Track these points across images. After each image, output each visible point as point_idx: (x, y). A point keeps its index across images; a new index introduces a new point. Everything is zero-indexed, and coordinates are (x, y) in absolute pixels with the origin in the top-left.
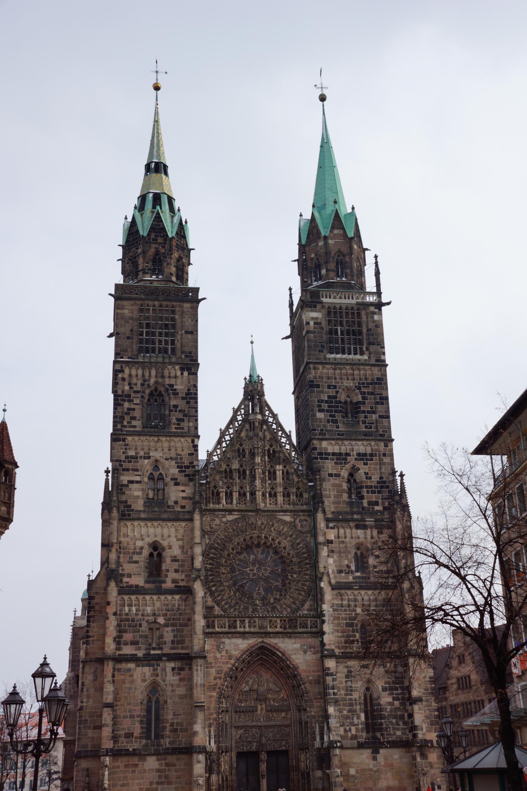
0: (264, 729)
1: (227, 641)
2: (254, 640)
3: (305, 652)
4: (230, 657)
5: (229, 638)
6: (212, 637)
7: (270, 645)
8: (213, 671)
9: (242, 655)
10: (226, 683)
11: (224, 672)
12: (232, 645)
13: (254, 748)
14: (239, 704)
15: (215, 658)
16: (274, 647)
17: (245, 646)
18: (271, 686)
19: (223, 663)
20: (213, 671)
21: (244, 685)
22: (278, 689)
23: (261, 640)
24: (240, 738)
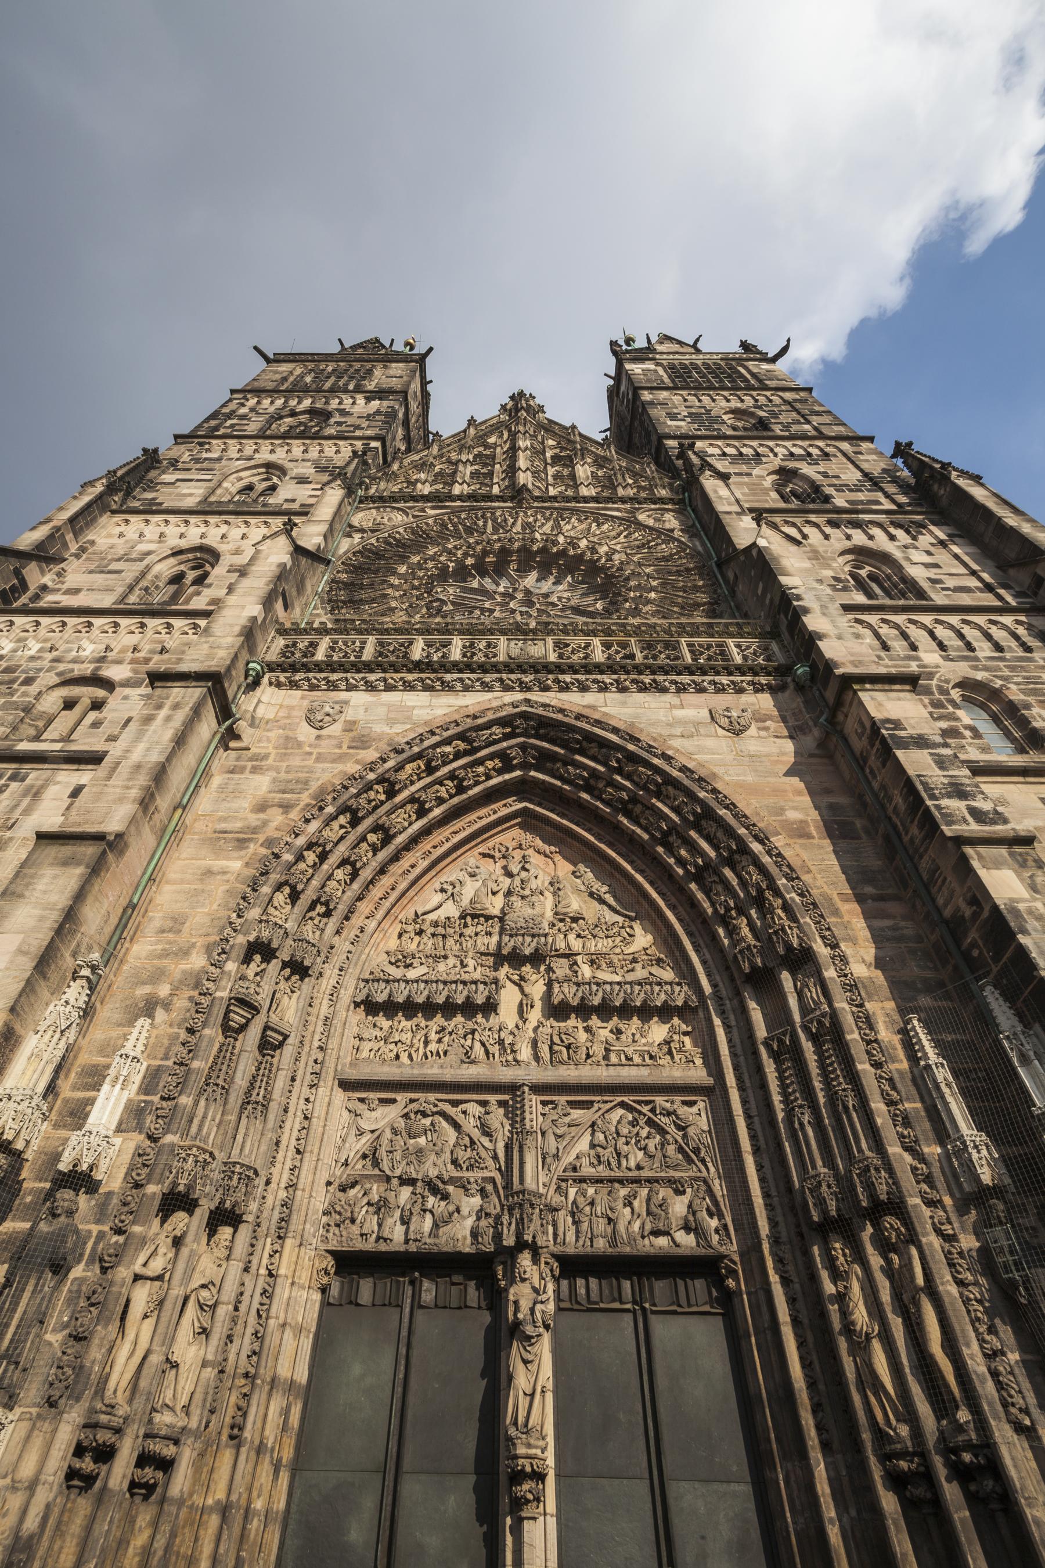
0: (533, 1102)
1: (360, 698)
2: (489, 695)
3: (737, 730)
4: (362, 742)
5: (371, 687)
6: (294, 685)
7: (561, 711)
8: (260, 785)
9: (421, 738)
10: (314, 826)
11: (314, 786)
12: (382, 711)
13: (460, 1235)
14: (396, 972)
15: (290, 743)
16: (579, 717)
17: (440, 712)
18: (575, 904)
19: (319, 758)
20: (260, 785)
21: (438, 898)
22: (620, 919)
23: (518, 696)
24: (371, 1156)
